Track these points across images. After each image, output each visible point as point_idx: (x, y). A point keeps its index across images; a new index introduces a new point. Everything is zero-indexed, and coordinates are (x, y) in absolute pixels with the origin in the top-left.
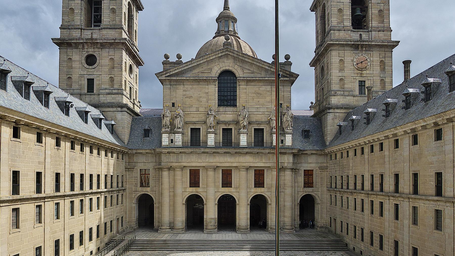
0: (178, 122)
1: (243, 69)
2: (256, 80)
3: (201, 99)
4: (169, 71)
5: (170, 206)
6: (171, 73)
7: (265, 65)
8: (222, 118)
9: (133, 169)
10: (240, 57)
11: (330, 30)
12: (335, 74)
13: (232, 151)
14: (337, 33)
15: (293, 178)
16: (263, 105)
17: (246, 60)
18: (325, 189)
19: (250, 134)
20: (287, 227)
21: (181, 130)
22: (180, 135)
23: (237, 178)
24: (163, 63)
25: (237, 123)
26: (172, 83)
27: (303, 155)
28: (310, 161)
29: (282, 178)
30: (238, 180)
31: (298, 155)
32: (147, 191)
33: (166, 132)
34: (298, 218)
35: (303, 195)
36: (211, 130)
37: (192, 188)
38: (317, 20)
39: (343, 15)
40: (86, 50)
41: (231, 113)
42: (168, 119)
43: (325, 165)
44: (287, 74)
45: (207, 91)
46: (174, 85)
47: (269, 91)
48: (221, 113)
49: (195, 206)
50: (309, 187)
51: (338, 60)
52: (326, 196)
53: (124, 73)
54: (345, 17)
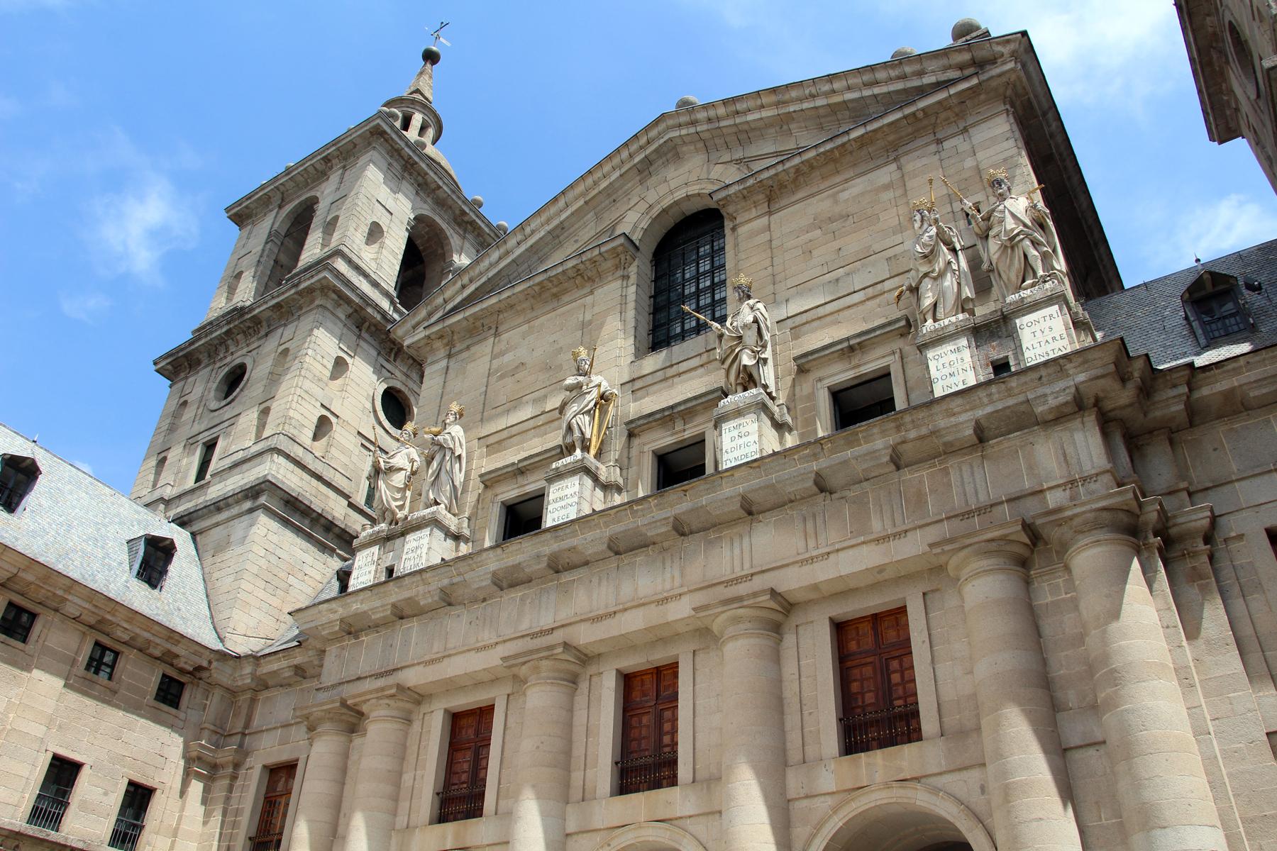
2: (810, 165)
6: (449, 307)
7: (842, 92)
9: (237, 766)
10: (723, 124)
16: (865, 256)
26: (459, 347)
27: (1221, 429)
31: (1172, 433)
40: (229, 359)
41: (695, 362)
42: (399, 479)
44: (961, 67)
45: (588, 317)
46: (461, 351)
47: (887, 187)
48: (649, 380)
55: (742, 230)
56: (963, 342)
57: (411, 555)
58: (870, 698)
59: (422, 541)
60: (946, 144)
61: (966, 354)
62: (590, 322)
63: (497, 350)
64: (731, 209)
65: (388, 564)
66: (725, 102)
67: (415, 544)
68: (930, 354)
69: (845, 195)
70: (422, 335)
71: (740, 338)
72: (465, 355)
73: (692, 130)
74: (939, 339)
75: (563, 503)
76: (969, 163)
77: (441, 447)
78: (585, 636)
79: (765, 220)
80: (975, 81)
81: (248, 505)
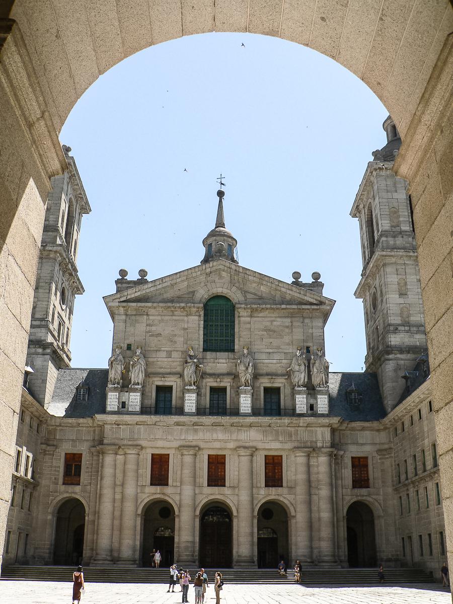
0: (137, 375)
1: (245, 292)
2: (267, 309)
3: (176, 339)
4: (126, 294)
5: (113, 518)
8: (209, 367)
11: (381, 236)
12: (393, 301)
13: (226, 420)
14: (391, 241)
15: (333, 470)
16: (278, 347)
17: (250, 278)
18: (390, 490)
19: (257, 395)
20: (326, 558)
21: (140, 386)
22: (139, 394)
23: (234, 469)
24: (117, 282)
25: (236, 376)
28: (360, 441)
29: (314, 470)
30: (236, 473)
32: (76, 492)
33: (115, 389)
34: (344, 545)
35: (352, 501)
36: (191, 388)
37: (153, 487)
38: (361, 228)
39: (399, 216)
41: (224, 361)
43: (386, 446)
45: (186, 327)
47: (287, 327)
49: (158, 516)
50: (361, 487)
51: (396, 280)
52: (393, 502)
53: (53, 297)
54: (401, 219)
55: (242, 319)
56: (305, 396)
57: (133, 400)
58: (270, 474)
59: (136, 397)
60: (307, 321)
61: (305, 400)
62: (186, 329)
63: (149, 322)
64: (240, 310)
65: (124, 400)
66: (244, 268)
67: (134, 397)
68: (297, 396)
69: (275, 323)
70: (117, 304)
71: (247, 368)
72: (133, 317)
73: (229, 270)
74: (299, 393)
75: (191, 401)
76: (310, 331)
77: (139, 363)
78: (202, 445)
79: (248, 319)
80: (318, 307)
81: (40, 350)
